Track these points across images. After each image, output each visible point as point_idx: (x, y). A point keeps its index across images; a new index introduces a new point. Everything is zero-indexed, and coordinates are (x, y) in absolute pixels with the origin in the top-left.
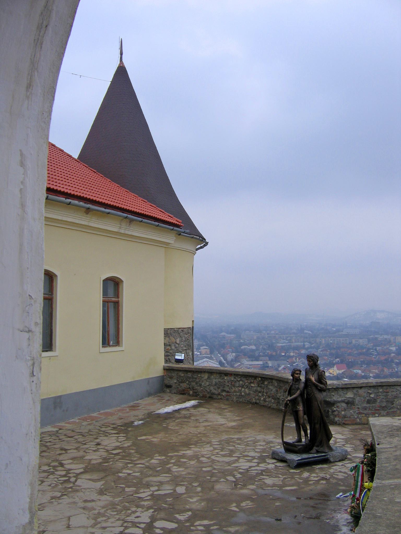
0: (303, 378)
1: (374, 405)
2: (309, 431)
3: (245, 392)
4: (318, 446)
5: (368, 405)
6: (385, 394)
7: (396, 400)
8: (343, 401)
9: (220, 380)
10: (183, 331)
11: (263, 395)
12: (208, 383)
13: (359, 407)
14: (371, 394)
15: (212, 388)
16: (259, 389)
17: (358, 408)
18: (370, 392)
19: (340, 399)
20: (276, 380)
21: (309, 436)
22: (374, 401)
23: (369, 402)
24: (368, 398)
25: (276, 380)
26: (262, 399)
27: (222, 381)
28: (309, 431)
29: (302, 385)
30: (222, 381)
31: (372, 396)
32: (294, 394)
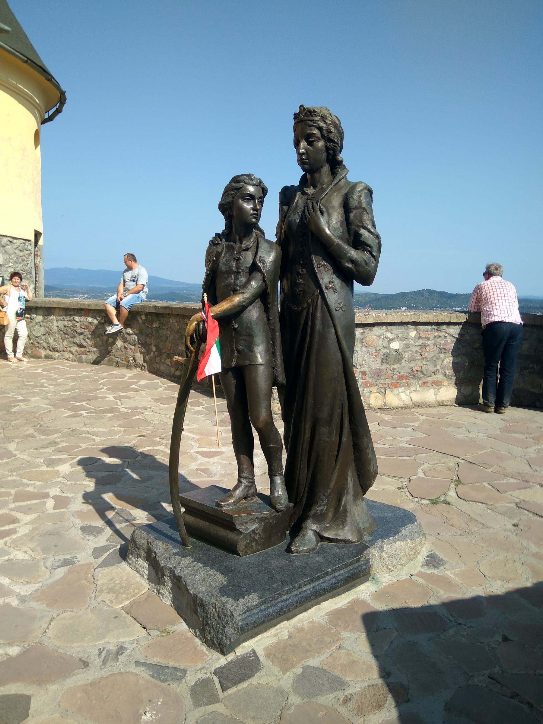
0: (269, 221)
1: (396, 366)
4: (319, 518)
5: (384, 367)
6: (421, 341)
7: (442, 356)
9: (66, 323)
10: (11, 242)
12: (42, 330)
13: (367, 370)
14: (392, 340)
15: (51, 340)
20: (176, 316)
22: (398, 357)
23: (386, 359)
25: (176, 316)
27: (70, 324)
29: (269, 258)
30: (70, 324)
31: (395, 345)
32: (235, 292)
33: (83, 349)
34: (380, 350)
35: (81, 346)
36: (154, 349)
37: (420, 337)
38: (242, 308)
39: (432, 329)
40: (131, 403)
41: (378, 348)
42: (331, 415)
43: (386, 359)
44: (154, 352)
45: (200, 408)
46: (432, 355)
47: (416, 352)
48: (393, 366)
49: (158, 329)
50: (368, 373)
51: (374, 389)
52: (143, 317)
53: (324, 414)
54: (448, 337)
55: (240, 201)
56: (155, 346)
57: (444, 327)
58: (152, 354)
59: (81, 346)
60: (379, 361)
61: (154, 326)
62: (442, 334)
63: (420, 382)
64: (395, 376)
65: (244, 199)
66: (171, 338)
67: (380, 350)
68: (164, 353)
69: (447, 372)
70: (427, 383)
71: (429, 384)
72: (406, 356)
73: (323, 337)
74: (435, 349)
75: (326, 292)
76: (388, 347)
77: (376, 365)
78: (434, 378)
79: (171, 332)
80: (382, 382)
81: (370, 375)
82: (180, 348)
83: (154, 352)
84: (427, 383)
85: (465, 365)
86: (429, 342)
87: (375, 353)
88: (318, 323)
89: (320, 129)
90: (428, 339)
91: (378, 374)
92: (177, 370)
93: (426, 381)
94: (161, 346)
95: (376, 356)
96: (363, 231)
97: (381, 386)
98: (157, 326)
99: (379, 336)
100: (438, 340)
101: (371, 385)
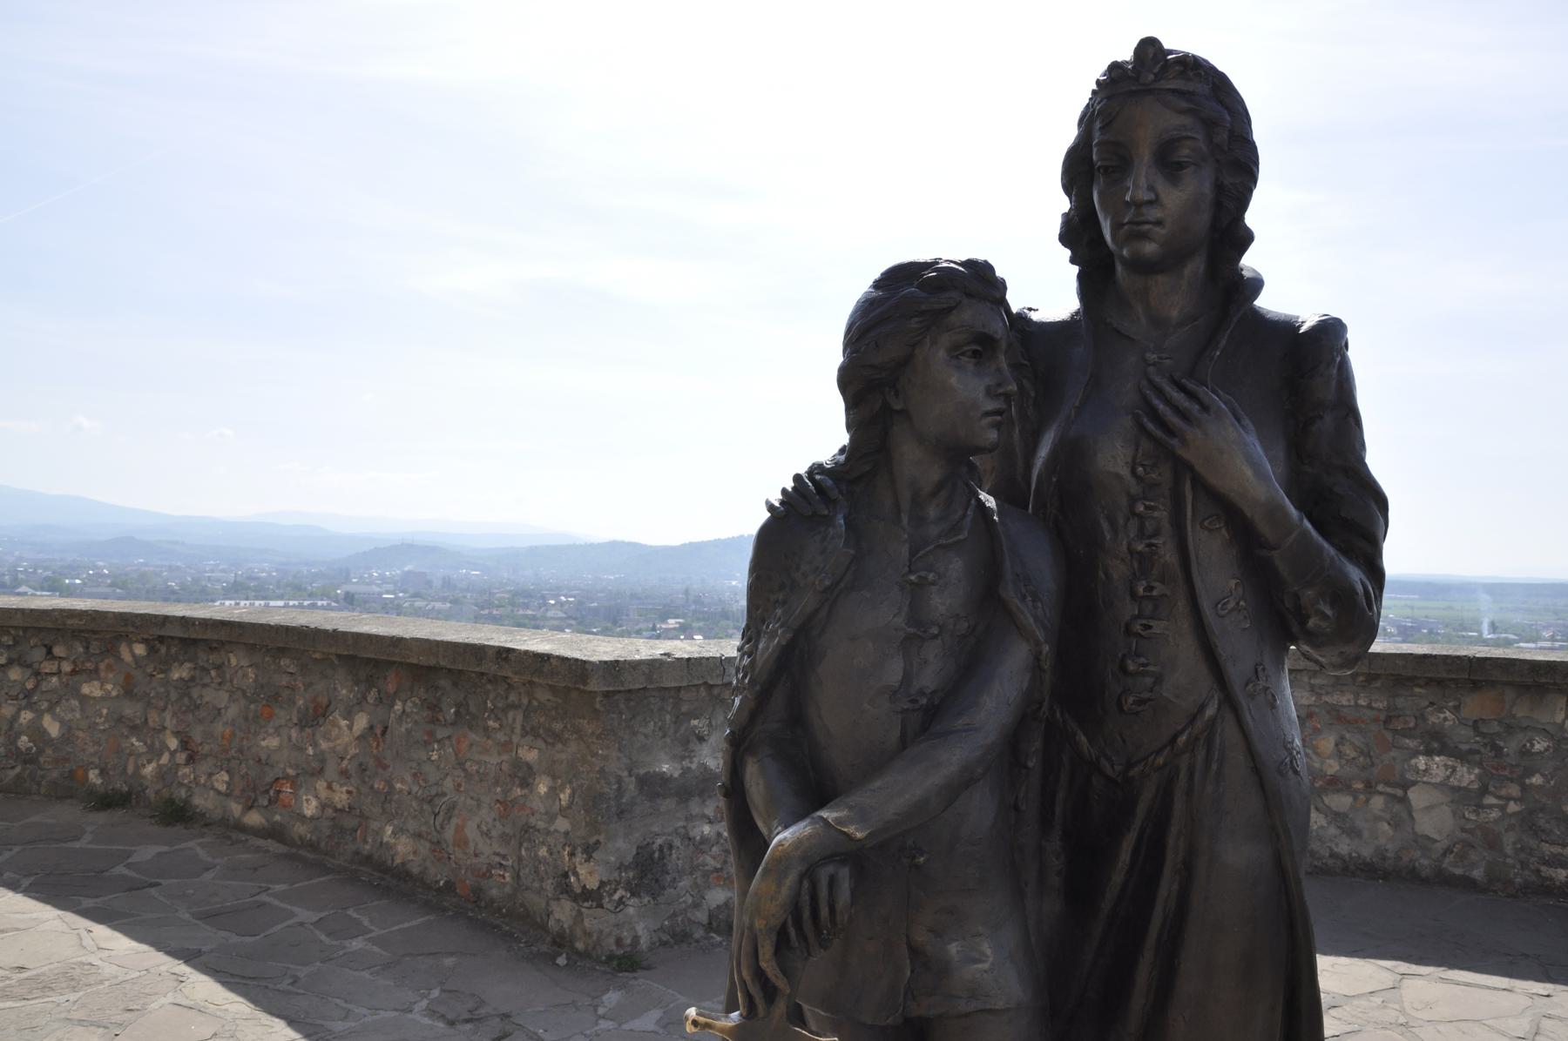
3: (38, 733)
11: (155, 752)
16: (130, 710)
26: (149, 770)
36: (173, 743)
44: (173, 754)
45: (357, 944)
49: (186, 685)
52: (140, 650)
55: (942, 354)
56: (176, 734)
58: (165, 759)
61: (176, 676)
66: (232, 712)
68: (206, 756)
79: (231, 693)
82: (264, 744)
83: (173, 754)
92: (250, 808)
94: (197, 735)
98: (184, 675)
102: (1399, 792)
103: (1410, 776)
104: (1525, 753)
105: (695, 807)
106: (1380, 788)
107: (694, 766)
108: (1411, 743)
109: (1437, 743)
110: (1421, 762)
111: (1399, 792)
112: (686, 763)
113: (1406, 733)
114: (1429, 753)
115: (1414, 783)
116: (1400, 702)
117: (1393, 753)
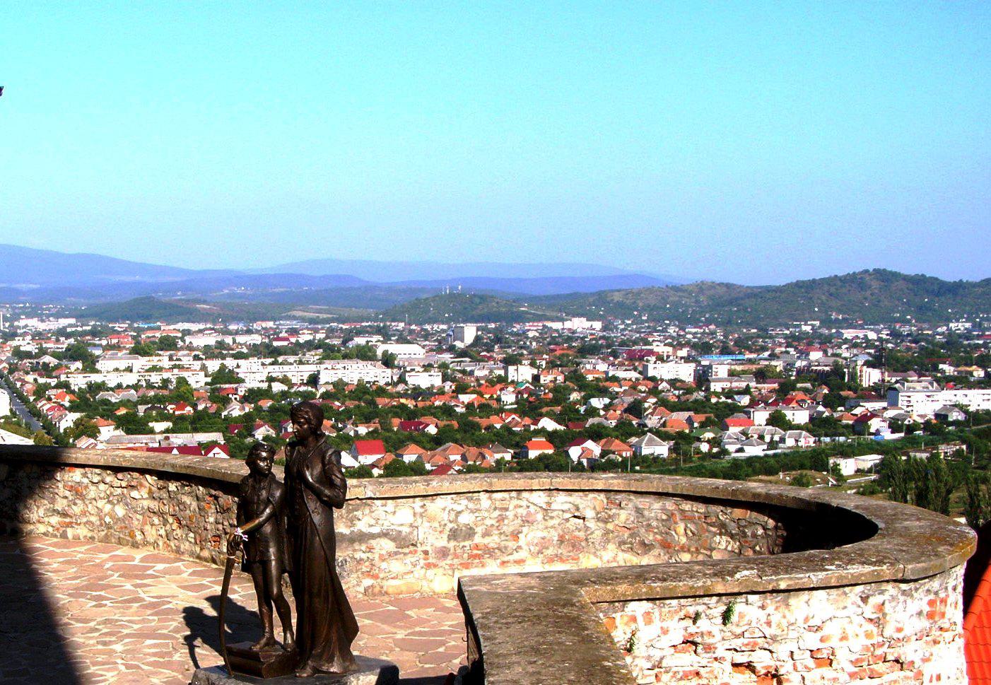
1: (467, 543)
2: (294, 621)
5: (452, 544)
6: (497, 513)
7: (525, 530)
8: (385, 535)
13: (428, 548)
14: (460, 512)
17: (426, 553)
18: (459, 508)
19: (376, 530)
21: (294, 629)
22: (470, 533)
24: (450, 526)
28: (294, 621)
33: (68, 520)
34: (445, 525)
35: (65, 515)
37: (495, 509)
38: (261, 525)
39: (511, 498)
40: (155, 591)
41: (443, 523)
42: (319, 591)
43: (454, 535)
46: (511, 529)
47: (492, 525)
48: (462, 544)
50: (430, 552)
51: (439, 571)
53: (315, 591)
54: (532, 506)
57: (525, 495)
59: (65, 515)
60: (445, 537)
62: (524, 503)
63: (499, 561)
64: (466, 555)
65: (261, 460)
67: (445, 525)
69: (532, 548)
70: (508, 562)
71: (509, 565)
72: (479, 530)
73: (312, 543)
74: (516, 522)
75: (312, 515)
76: (455, 521)
77: (442, 542)
78: (516, 556)
80: (449, 562)
81: (433, 555)
84: (508, 562)
85: (553, 541)
86: (507, 513)
87: (439, 529)
88: (309, 533)
89: (305, 418)
90: (507, 509)
91: (443, 553)
93: (506, 559)
95: (440, 532)
96: (334, 477)
97: (447, 567)
99: (444, 509)
100: (520, 511)
101: (435, 566)
102: (708, 553)
103: (713, 545)
104: (754, 535)
105: (356, 546)
106: (702, 551)
107: (356, 531)
108: (714, 529)
109: (723, 529)
110: (717, 538)
111: (708, 553)
112: (352, 529)
113: (712, 525)
114: (721, 534)
115: (715, 549)
116: (709, 509)
117: (707, 534)
